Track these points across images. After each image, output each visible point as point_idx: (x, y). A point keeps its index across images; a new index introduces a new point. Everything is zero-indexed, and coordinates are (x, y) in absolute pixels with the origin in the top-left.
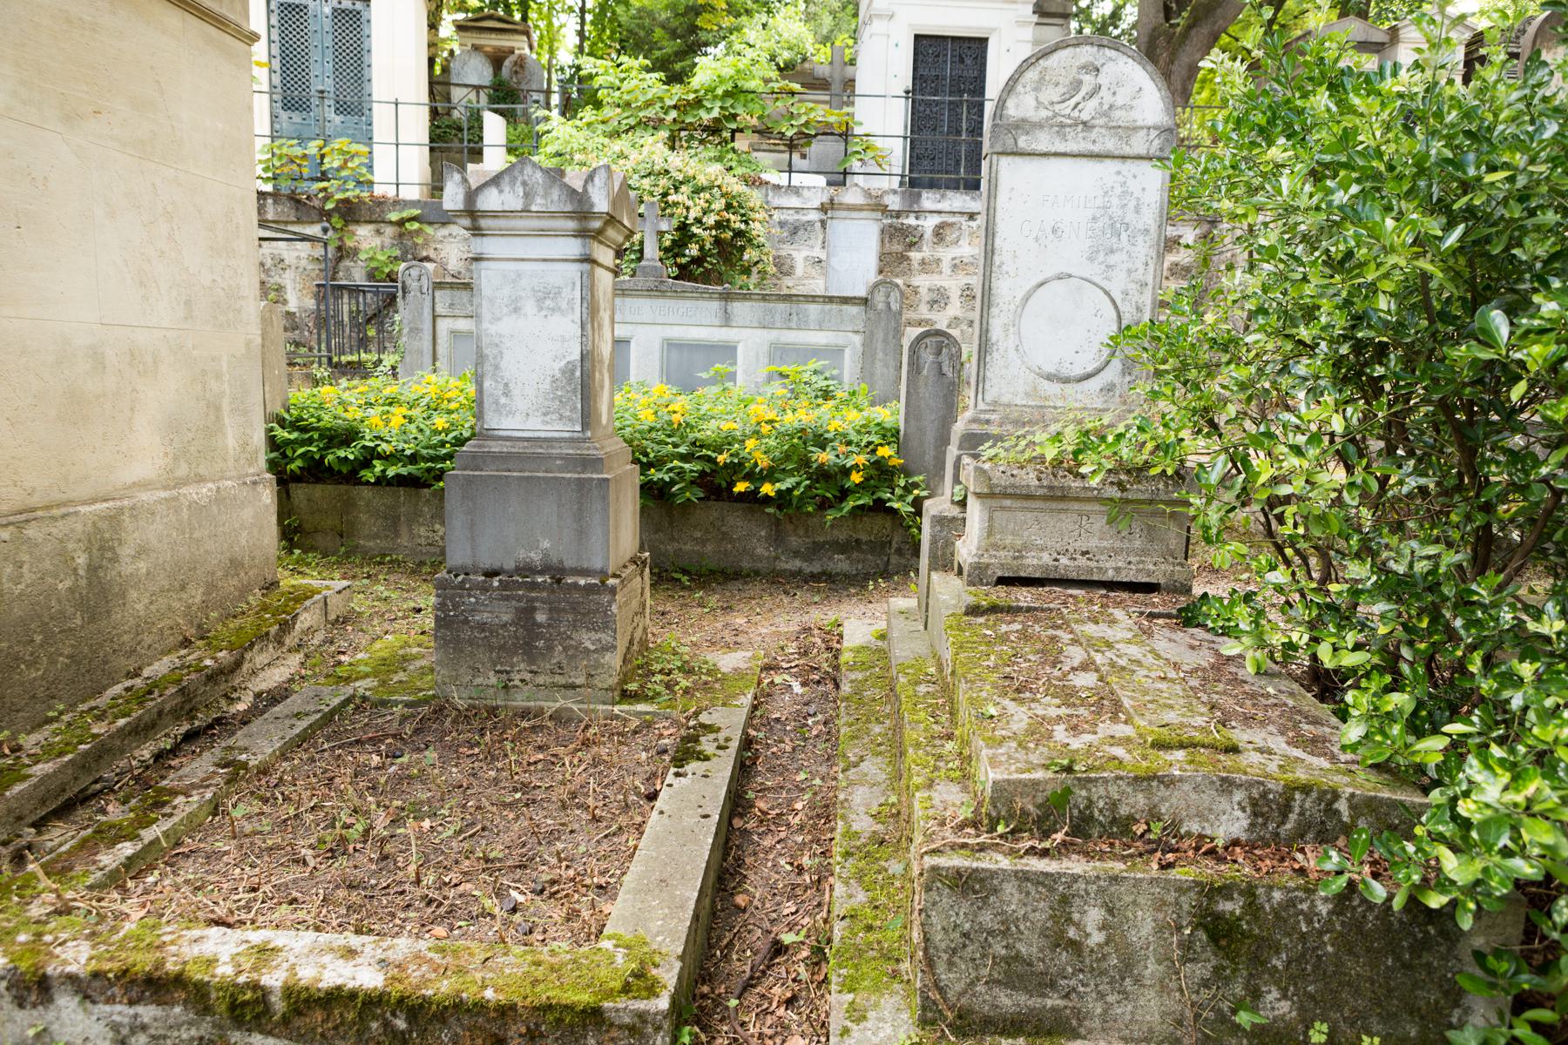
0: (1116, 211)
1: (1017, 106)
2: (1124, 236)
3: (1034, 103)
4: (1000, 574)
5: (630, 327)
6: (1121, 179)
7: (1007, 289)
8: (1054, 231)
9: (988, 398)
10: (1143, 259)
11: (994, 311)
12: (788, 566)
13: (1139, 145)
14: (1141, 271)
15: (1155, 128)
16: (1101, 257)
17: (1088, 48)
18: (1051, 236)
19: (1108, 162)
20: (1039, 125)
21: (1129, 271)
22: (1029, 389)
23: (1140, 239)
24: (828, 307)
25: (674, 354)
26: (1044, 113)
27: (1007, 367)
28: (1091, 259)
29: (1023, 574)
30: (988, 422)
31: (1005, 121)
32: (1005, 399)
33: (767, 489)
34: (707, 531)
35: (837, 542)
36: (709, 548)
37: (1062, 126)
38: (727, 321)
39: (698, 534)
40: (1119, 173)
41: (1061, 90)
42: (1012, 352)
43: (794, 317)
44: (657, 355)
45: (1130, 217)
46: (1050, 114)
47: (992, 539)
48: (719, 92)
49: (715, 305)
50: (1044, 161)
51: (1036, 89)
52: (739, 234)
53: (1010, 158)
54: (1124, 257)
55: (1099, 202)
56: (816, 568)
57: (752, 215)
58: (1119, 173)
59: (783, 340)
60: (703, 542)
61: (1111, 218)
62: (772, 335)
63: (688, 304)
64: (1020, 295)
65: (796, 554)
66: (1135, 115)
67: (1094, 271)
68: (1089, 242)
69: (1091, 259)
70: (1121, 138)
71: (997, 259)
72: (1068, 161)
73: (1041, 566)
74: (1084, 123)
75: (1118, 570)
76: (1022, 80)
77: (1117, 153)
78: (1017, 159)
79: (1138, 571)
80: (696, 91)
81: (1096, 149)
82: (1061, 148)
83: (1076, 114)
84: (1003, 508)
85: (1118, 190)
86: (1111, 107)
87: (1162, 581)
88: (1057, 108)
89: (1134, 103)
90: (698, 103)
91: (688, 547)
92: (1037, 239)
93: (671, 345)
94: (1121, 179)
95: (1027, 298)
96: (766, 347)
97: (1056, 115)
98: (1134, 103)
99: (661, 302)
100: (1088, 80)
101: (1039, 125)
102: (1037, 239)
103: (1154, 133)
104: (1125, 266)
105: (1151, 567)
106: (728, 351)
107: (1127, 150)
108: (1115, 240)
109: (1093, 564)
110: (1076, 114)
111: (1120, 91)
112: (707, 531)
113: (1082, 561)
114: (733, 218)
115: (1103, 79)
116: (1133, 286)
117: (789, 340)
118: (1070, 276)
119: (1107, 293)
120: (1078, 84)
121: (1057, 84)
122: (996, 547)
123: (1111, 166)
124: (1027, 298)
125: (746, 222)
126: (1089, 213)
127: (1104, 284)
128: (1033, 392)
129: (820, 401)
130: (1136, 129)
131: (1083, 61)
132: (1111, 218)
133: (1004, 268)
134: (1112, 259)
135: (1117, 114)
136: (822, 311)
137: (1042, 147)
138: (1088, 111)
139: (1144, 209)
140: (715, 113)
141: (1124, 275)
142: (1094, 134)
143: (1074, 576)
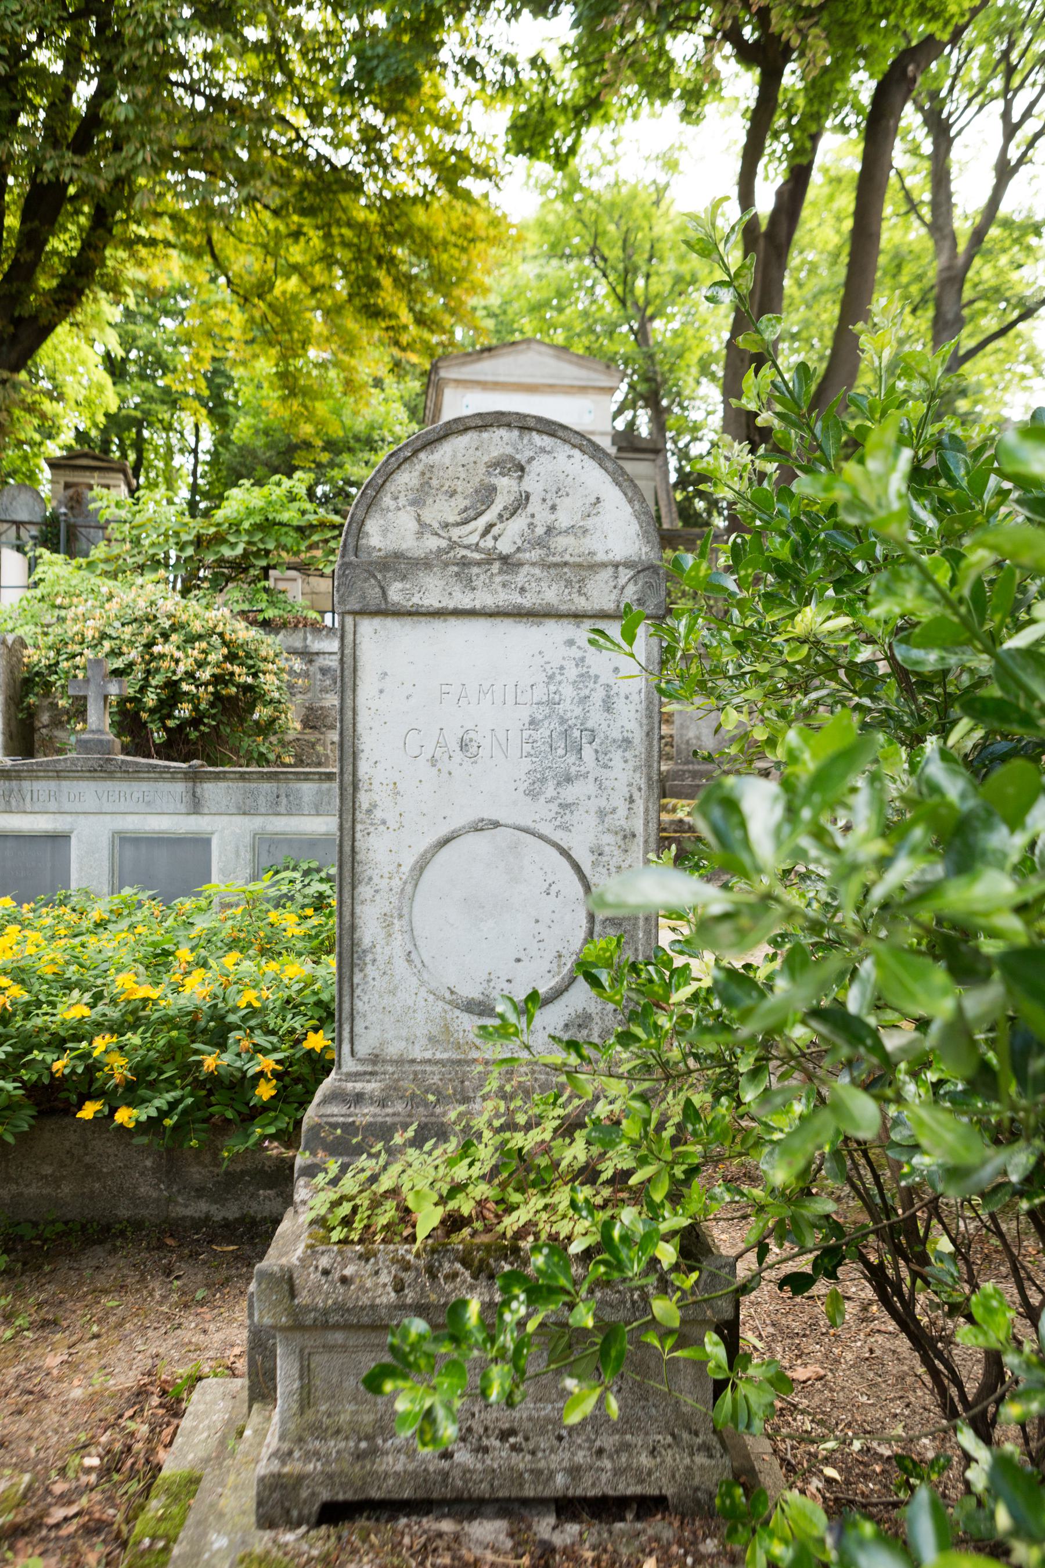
0: (570, 709)
1: (385, 531)
2: (588, 752)
3: (413, 526)
4: (325, 1495)
5: (69, 818)
6: (574, 652)
7: (384, 852)
8: (463, 746)
9: (363, 1049)
10: (625, 791)
11: (364, 891)
12: (188, 1212)
13: (601, 593)
14: (622, 812)
15: (628, 564)
16: (550, 791)
17: (503, 432)
18: (458, 756)
19: (551, 625)
20: (425, 564)
21: (602, 814)
22: (435, 1031)
23: (617, 756)
24: (325, 786)
25: (129, 852)
26: (433, 543)
27: (393, 992)
28: (532, 794)
29: (375, 1494)
30: (359, 1098)
31: (364, 557)
32: (393, 1050)
33: (124, 1116)
34: (62, 1165)
35: (262, 1172)
36: (66, 1189)
37: (465, 563)
38: (196, 806)
39: (47, 1170)
40: (571, 643)
41: (461, 502)
42: (400, 965)
43: (284, 800)
44: (106, 853)
45: (596, 718)
46: (444, 543)
47: (310, 1415)
48: (246, 525)
49: (180, 787)
50: (438, 624)
51: (414, 503)
52: (247, 688)
53: (377, 622)
54: (591, 788)
55: (540, 694)
56: (232, 1212)
57: (263, 666)
58: (571, 643)
59: (270, 828)
60: (56, 1181)
61: (563, 721)
62: (256, 823)
63: (145, 786)
64: (409, 860)
65: (200, 1192)
66: (589, 543)
67: (538, 814)
68: (526, 764)
69: (532, 794)
70: (569, 583)
71: (364, 799)
72: (481, 625)
73: (414, 1475)
74: (504, 559)
75: (574, 1472)
76: (390, 487)
77: (564, 608)
78: (390, 623)
79: (617, 1472)
80: (218, 525)
81: (527, 601)
82: (464, 600)
83: (488, 543)
84: (330, 1348)
85: (572, 672)
86: (549, 530)
87: (669, 1491)
88: (455, 533)
89: (589, 523)
90: (219, 539)
91: (33, 1190)
92: (433, 761)
93: (124, 840)
94: (574, 652)
95: (421, 866)
96: (248, 840)
97: (453, 545)
98: (589, 523)
99: (109, 784)
100: (506, 486)
101: (425, 564)
102: (433, 761)
103: (625, 574)
104: (593, 805)
105: (645, 1460)
106: (202, 843)
107: (581, 604)
108: (572, 758)
109: (521, 1462)
110: (488, 543)
111: (564, 504)
112: (62, 1165)
113: (500, 1455)
114: (237, 670)
115: (530, 484)
116: (608, 838)
117: (278, 829)
118: (496, 824)
119: (565, 853)
120: (487, 494)
121: (453, 494)
122: (318, 1431)
123: (556, 632)
124: (421, 866)
125: (255, 675)
126: (524, 714)
127: (557, 836)
128: (442, 1036)
129: (309, 912)
130: (594, 567)
131: (495, 453)
132: (563, 721)
133: (378, 814)
134: (571, 793)
135: (561, 542)
136: (319, 791)
137: (432, 600)
138: (510, 536)
139: (620, 705)
140: (239, 550)
141: (592, 820)
142: (521, 579)
143: (483, 1489)
